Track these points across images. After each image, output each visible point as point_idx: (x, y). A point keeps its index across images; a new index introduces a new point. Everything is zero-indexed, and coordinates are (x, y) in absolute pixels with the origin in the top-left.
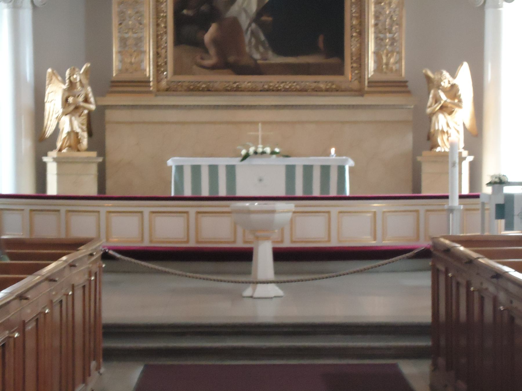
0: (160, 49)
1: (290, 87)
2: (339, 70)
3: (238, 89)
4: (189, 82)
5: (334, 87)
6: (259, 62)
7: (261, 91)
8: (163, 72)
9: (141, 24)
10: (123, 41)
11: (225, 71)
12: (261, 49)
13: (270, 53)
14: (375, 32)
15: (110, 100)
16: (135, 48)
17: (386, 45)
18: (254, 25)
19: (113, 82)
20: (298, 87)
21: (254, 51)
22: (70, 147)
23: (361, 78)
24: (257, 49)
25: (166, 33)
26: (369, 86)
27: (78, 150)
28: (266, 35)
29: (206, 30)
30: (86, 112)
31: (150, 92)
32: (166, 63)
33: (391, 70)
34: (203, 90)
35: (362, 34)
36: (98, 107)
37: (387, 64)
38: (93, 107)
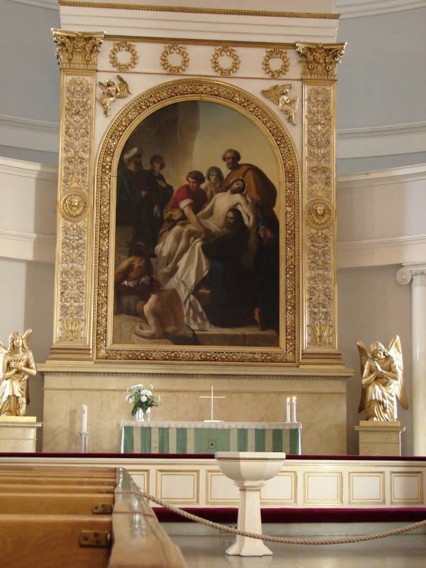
0: (100, 318)
1: (227, 357)
2: (274, 342)
3: (176, 358)
5: (269, 358)
6: (196, 332)
7: (198, 360)
8: (102, 340)
9: (83, 293)
10: (64, 310)
11: (164, 340)
12: (199, 320)
13: (208, 325)
14: (309, 307)
15: (50, 365)
16: (76, 317)
17: (320, 319)
18: (192, 297)
19: (51, 349)
20: (234, 357)
21: (192, 321)
22: (8, 411)
24: (195, 320)
26: (302, 358)
27: (17, 415)
28: (204, 307)
29: (146, 301)
30: (26, 377)
33: (325, 343)
34: (142, 359)
35: (295, 308)
36: (38, 372)
37: (320, 337)
38: (34, 372)
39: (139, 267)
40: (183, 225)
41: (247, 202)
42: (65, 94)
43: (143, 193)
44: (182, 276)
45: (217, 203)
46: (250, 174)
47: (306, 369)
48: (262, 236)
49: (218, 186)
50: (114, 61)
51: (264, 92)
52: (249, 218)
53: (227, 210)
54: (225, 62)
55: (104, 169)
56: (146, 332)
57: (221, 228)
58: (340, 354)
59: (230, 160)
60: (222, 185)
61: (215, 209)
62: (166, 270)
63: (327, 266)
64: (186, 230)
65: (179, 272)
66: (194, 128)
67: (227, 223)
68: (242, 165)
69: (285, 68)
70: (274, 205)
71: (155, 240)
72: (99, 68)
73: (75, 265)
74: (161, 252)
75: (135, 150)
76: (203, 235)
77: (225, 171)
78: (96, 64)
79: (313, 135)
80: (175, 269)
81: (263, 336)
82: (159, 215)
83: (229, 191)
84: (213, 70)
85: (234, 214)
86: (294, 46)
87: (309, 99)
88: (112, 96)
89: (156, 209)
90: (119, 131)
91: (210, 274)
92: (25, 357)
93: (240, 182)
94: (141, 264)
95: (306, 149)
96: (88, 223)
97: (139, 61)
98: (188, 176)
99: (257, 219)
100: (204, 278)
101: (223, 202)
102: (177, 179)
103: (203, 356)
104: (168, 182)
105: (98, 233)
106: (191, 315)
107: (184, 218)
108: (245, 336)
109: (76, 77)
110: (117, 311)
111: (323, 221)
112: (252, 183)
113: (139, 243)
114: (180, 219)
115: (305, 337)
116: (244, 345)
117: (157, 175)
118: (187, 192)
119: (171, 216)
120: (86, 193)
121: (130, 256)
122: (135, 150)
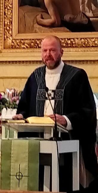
0: (6, 10)
4: (30, 40)
6: (91, 19)
7: (93, 46)
11: (62, 28)
21: (86, 8)
24: (90, 8)
56: (47, 21)
103: (96, 42)
106: (86, 3)
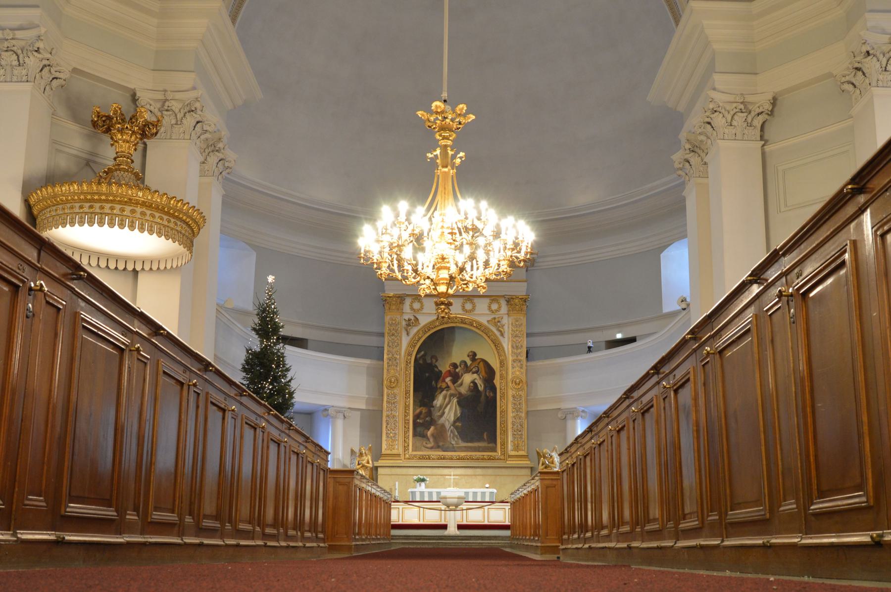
2: (494, 450)
3: (444, 459)
6: (454, 445)
12: (456, 439)
13: (460, 441)
18: (452, 427)
23: (504, 453)
24: (454, 440)
25: (409, 431)
29: (429, 429)
30: (369, 468)
31: (400, 460)
32: (408, 446)
34: (427, 459)
39: (425, 413)
40: (447, 391)
41: (480, 378)
42: (387, 325)
43: (427, 375)
44: (447, 417)
45: (464, 378)
46: (481, 364)
47: (510, 462)
48: (488, 395)
49: (465, 370)
50: (412, 309)
51: (488, 321)
52: (481, 386)
53: (470, 382)
54: (468, 306)
55: (408, 363)
56: (429, 445)
57: (467, 392)
58: (527, 456)
59: (471, 357)
60: (467, 369)
61: (464, 382)
62: (439, 414)
63: (521, 410)
64: (449, 393)
65: (445, 415)
66: (453, 341)
67: (470, 389)
68: (478, 359)
69: (500, 307)
70: (494, 379)
71: (433, 398)
72: (404, 311)
73: (392, 412)
74: (436, 405)
75: (423, 353)
76: (458, 396)
77: (469, 362)
78: (402, 309)
79: (514, 343)
80: (443, 413)
81: (489, 447)
82: (435, 385)
83: (471, 373)
84: (462, 310)
85: (474, 384)
86: (503, 296)
87: (512, 324)
88: (410, 326)
89: (433, 382)
90: (414, 343)
91: (462, 414)
92: (367, 458)
93: (476, 368)
94: (426, 411)
95: (510, 350)
96: (400, 391)
97: (424, 307)
98: (450, 366)
99: (485, 387)
100: (458, 417)
101: (468, 378)
102: (444, 366)
104: (440, 369)
105: (404, 396)
107: (448, 387)
108: (479, 447)
109: (392, 316)
110: (415, 435)
111: (519, 387)
112: (483, 368)
113: (425, 400)
114: (445, 388)
115: (510, 447)
116: (479, 451)
117: (434, 365)
118: (449, 373)
119: (441, 386)
120: (398, 376)
121: (420, 407)
122: (423, 353)
